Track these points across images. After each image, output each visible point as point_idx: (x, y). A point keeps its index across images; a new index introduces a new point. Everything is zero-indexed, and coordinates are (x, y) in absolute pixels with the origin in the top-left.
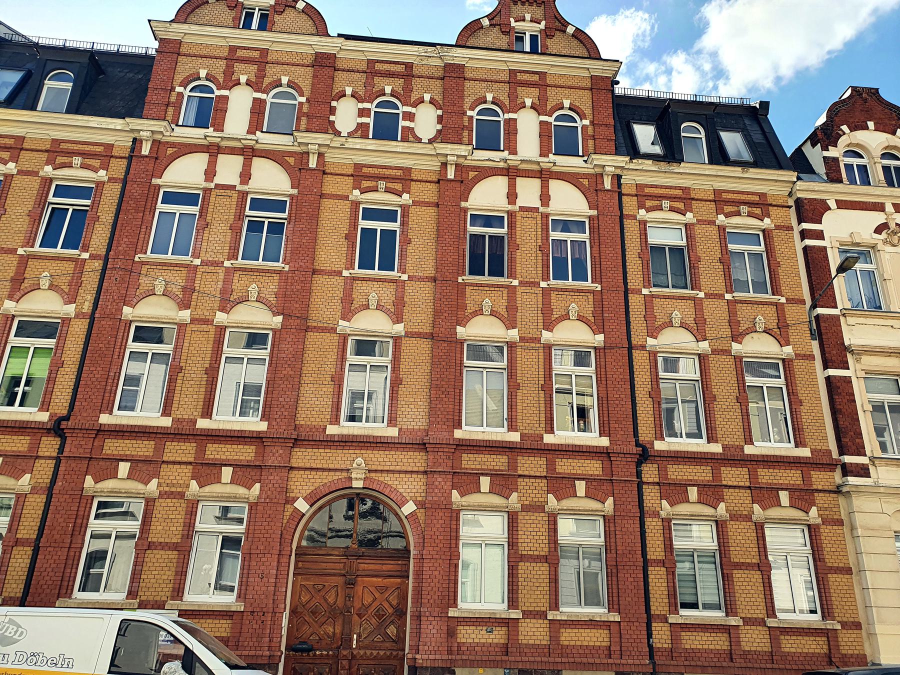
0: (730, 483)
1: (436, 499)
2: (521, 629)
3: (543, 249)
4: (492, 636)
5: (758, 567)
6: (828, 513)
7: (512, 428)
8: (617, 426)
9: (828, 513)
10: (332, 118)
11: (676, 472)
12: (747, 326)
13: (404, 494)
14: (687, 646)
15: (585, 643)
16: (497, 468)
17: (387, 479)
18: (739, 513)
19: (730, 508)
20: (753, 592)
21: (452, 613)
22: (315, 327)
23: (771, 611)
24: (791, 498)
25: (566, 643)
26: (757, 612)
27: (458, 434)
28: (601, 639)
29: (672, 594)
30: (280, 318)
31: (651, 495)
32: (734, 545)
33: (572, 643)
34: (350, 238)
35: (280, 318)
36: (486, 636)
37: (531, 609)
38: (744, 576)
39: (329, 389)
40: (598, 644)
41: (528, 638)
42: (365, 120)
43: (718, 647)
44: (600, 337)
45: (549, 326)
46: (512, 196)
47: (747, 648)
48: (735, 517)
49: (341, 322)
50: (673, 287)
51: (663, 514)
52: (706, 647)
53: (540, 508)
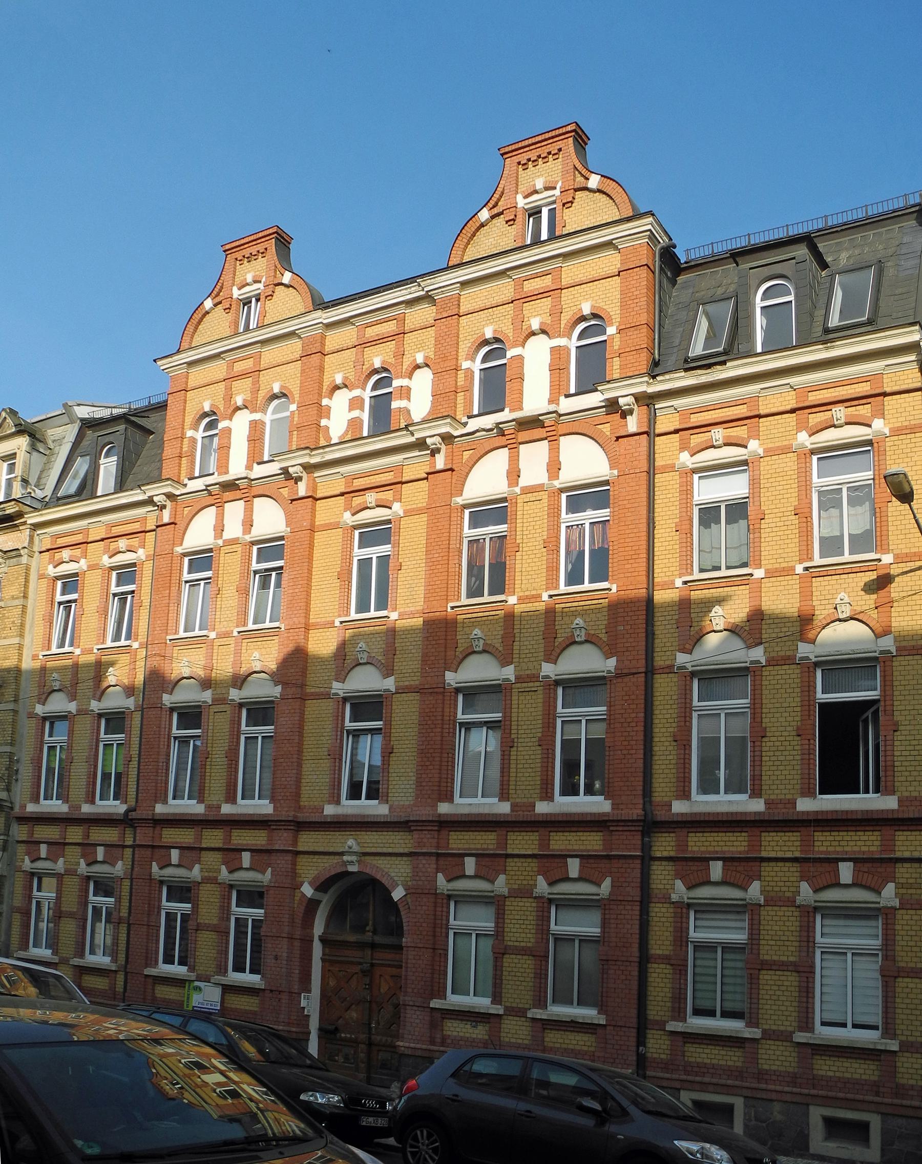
0: (773, 855)
1: (420, 883)
2: (503, 1026)
3: (551, 545)
4: (476, 1031)
5: (795, 968)
6: (913, 891)
7: (504, 796)
8: (621, 784)
9: (913, 891)
10: (324, 422)
11: (698, 843)
12: (826, 612)
13: (396, 878)
14: (692, 1060)
15: (571, 1047)
16: (485, 846)
17: (381, 862)
18: (781, 894)
19: (768, 889)
20: (784, 998)
21: (435, 1003)
22: (312, 694)
23: (806, 1024)
24: (856, 871)
25: (551, 1045)
26: (785, 1023)
27: (444, 808)
28: (589, 1044)
29: (678, 998)
30: (279, 689)
31: (661, 874)
32: (767, 937)
33: (558, 1045)
34: (344, 576)
35: (279, 689)
36: (471, 1031)
37: (514, 1005)
38: (775, 978)
39: (326, 764)
40: (585, 1048)
41: (510, 1035)
42: (356, 413)
43: (729, 1063)
44: (612, 663)
45: (552, 656)
46: (514, 474)
47: (766, 1067)
48: (771, 901)
49: (336, 685)
50: (728, 568)
51: (674, 897)
52: (714, 1061)
53: (524, 892)
